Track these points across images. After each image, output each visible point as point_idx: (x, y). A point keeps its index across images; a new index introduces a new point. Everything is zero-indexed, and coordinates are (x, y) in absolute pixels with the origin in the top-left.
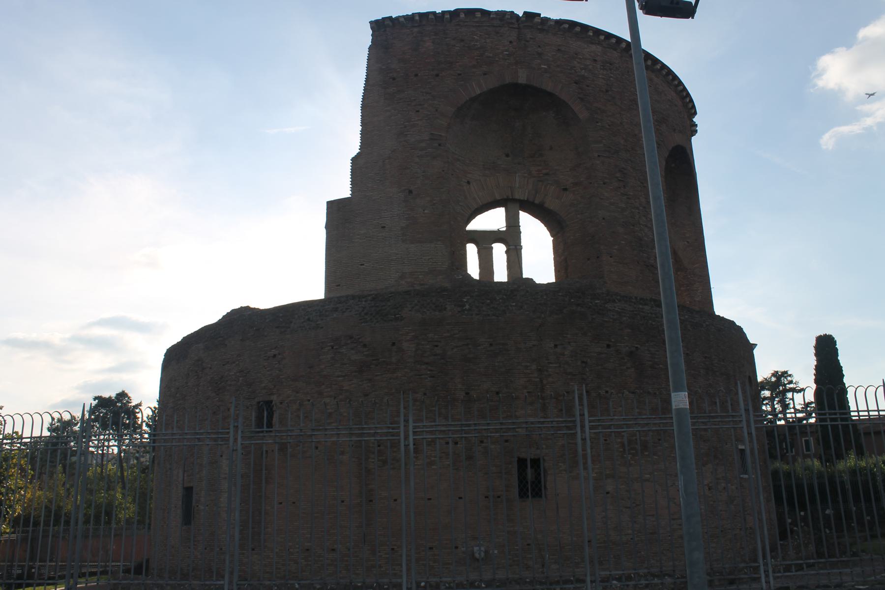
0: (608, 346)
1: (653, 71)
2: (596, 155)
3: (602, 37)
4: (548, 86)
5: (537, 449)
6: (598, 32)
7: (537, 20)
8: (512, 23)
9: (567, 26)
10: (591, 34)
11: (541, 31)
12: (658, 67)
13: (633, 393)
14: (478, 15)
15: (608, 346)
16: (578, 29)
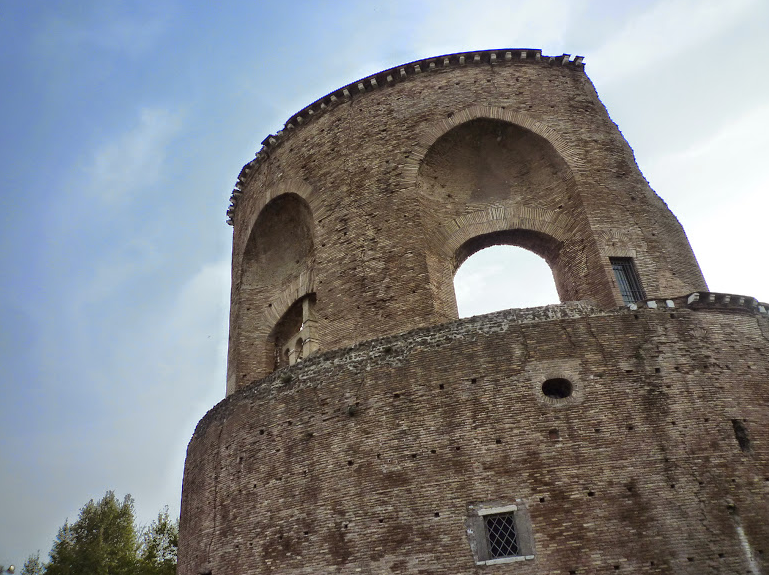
0: (262, 432)
1: (403, 80)
2: (317, 222)
3: (323, 106)
4: (282, 189)
5: (209, 562)
6: (315, 106)
7: (272, 140)
8: (263, 158)
9: (290, 126)
10: (311, 112)
11: (279, 146)
12: (403, 72)
13: (281, 479)
14: (247, 170)
15: (262, 432)
16: (299, 119)
